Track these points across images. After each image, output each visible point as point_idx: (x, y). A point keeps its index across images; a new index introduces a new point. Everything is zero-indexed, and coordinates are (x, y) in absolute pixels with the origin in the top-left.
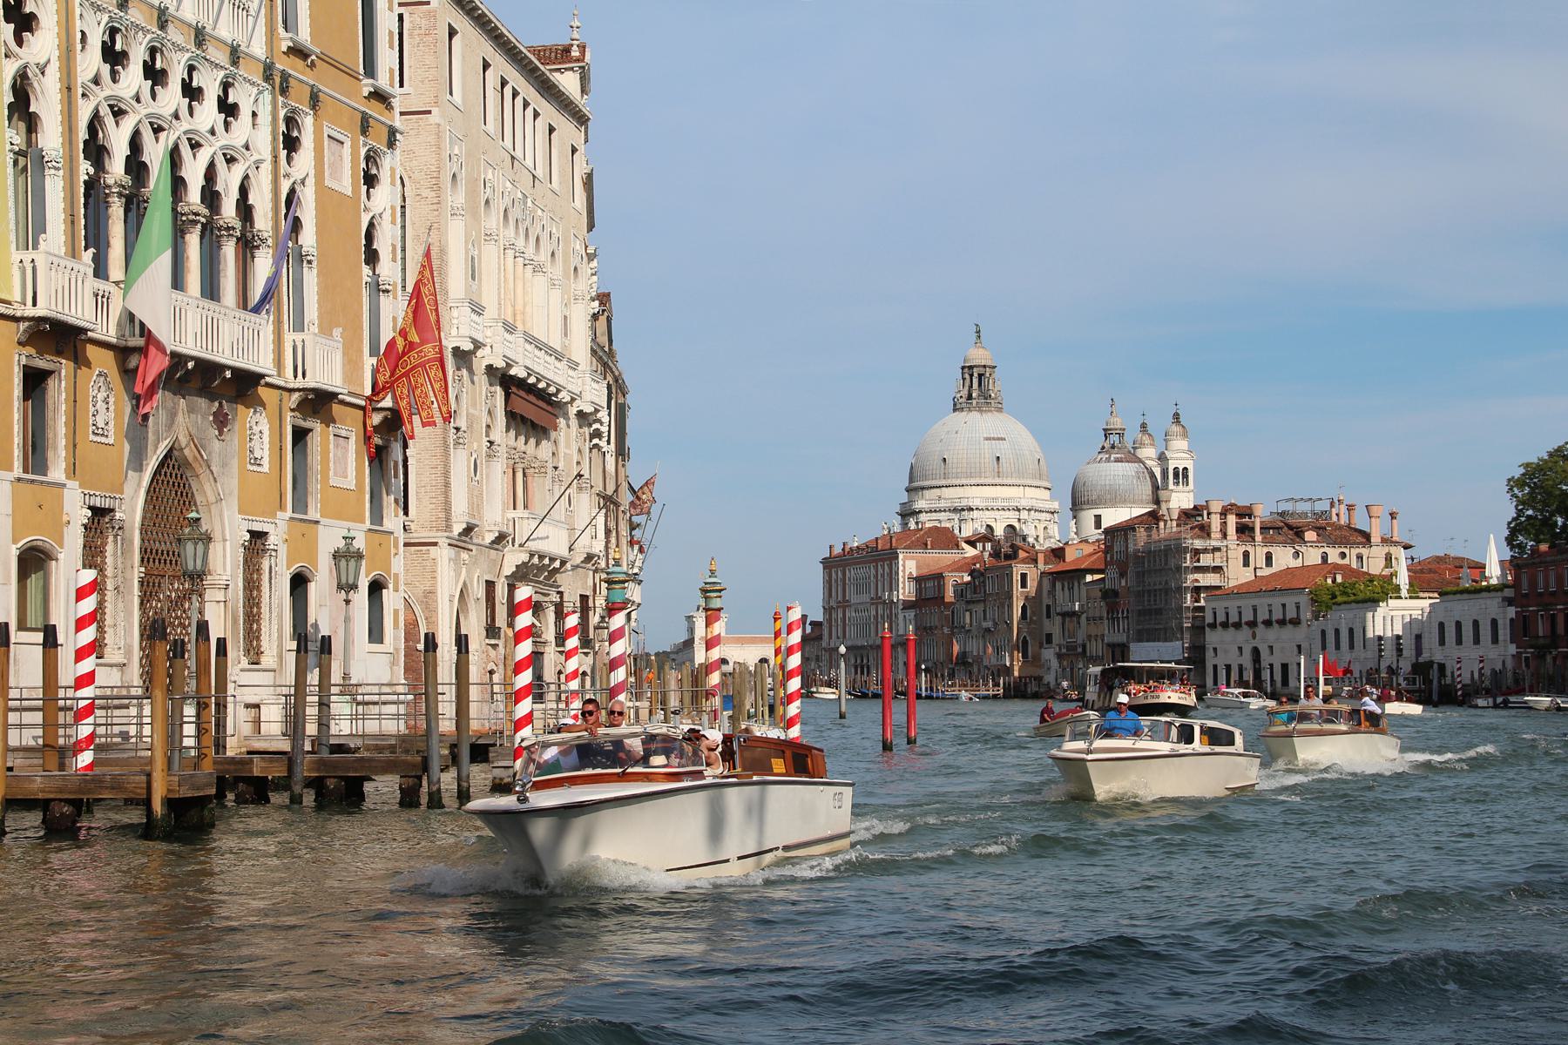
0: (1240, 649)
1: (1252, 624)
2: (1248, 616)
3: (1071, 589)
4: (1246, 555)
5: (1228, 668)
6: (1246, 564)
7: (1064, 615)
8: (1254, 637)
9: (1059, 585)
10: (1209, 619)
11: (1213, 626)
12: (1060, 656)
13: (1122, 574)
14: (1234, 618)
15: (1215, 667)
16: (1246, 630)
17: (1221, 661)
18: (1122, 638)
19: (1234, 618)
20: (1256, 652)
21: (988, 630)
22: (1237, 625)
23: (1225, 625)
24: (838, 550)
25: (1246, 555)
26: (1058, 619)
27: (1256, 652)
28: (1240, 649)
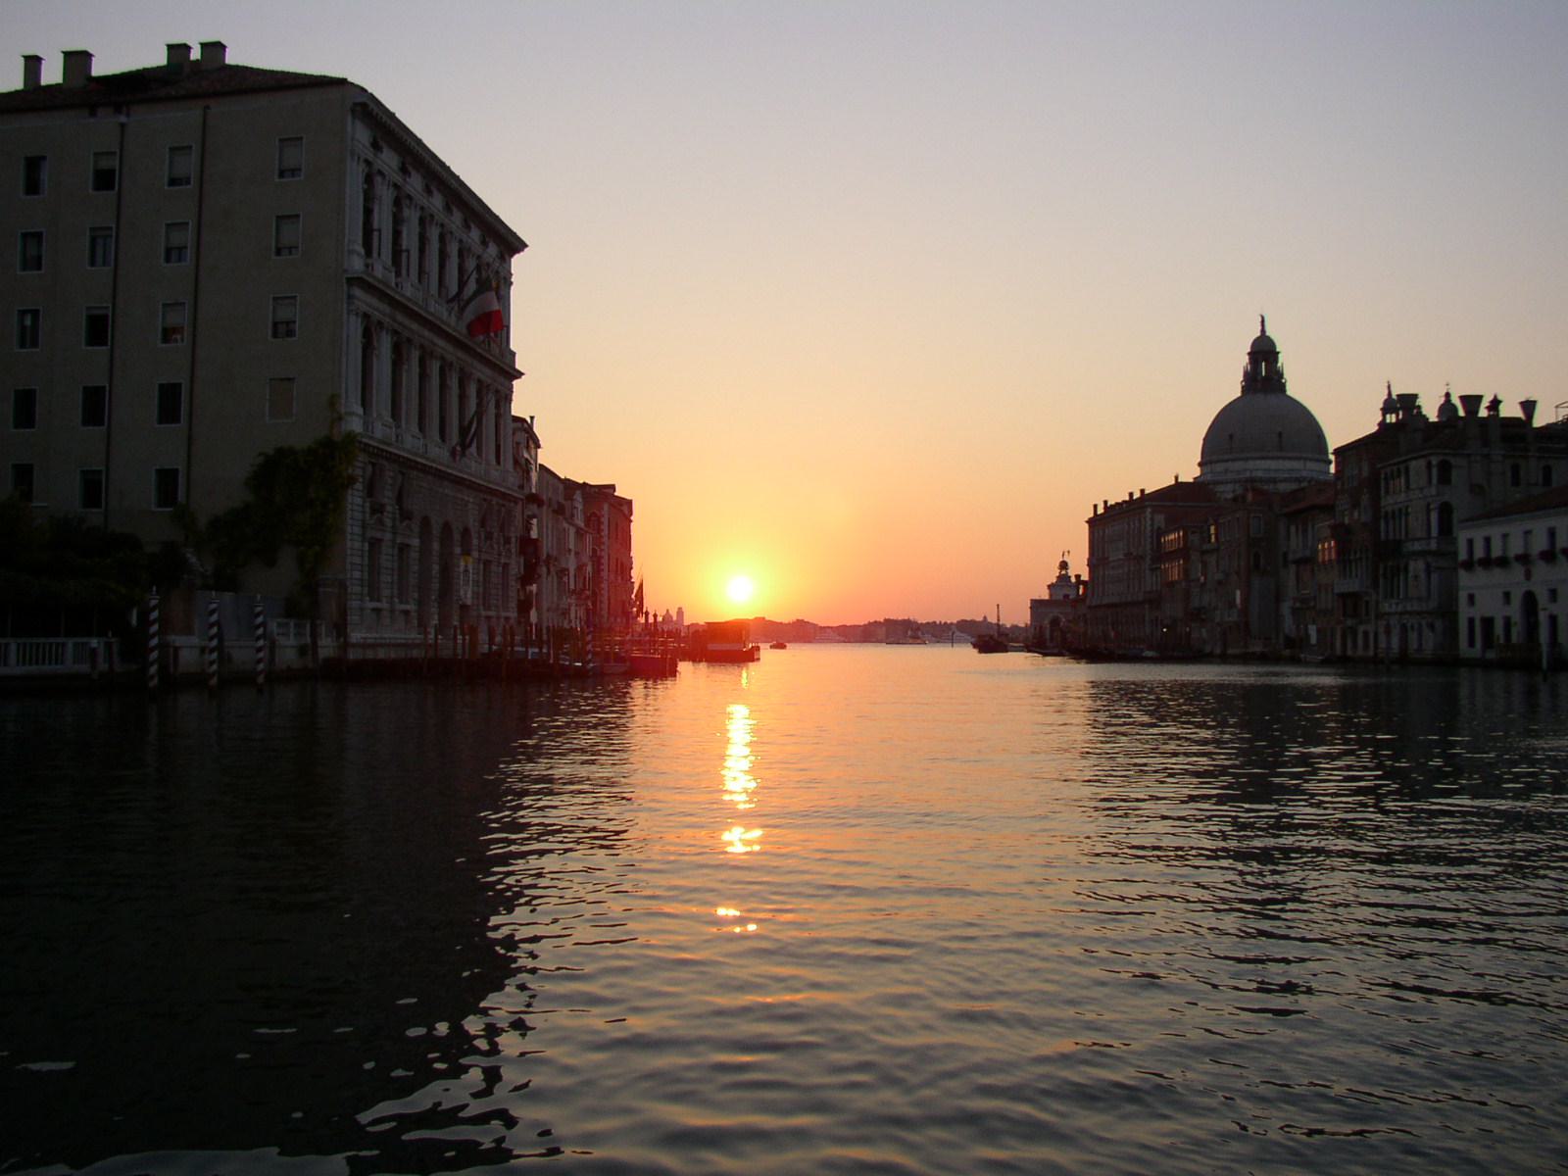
0: (1507, 596)
1: (1524, 559)
2: (1516, 547)
3: (1305, 531)
4: (1515, 470)
5: (1488, 622)
6: (1516, 482)
7: (1298, 562)
8: (1528, 575)
9: (1293, 529)
10: (1463, 556)
11: (1468, 565)
12: (1294, 611)
13: (1355, 505)
14: (1496, 552)
15: (1471, 621)
16: (1518, 571)
17: (1479, 612)
18: (1352, 585)
19: (1496, 552)
20: (1530, 599)
21: (1220, 583)
22: (1503, 562)
23: (1487, 562)
24: (1100, 511)
25: (1515, 470)
26: (1293, 568)
27: (1530, 599)
28: (1507, 596)
